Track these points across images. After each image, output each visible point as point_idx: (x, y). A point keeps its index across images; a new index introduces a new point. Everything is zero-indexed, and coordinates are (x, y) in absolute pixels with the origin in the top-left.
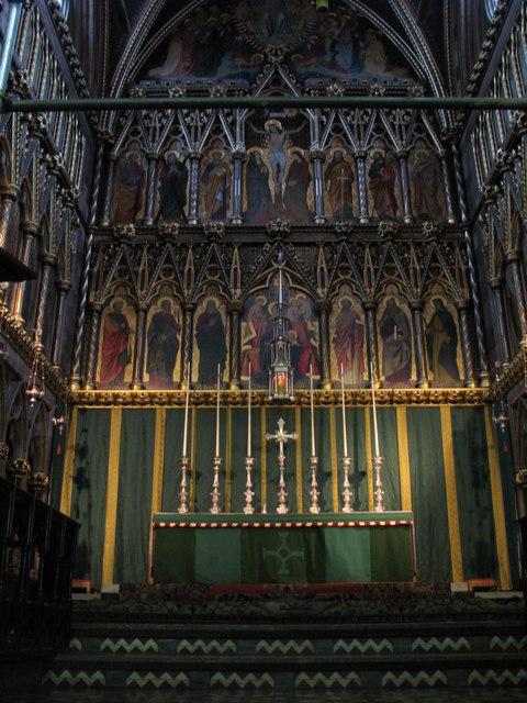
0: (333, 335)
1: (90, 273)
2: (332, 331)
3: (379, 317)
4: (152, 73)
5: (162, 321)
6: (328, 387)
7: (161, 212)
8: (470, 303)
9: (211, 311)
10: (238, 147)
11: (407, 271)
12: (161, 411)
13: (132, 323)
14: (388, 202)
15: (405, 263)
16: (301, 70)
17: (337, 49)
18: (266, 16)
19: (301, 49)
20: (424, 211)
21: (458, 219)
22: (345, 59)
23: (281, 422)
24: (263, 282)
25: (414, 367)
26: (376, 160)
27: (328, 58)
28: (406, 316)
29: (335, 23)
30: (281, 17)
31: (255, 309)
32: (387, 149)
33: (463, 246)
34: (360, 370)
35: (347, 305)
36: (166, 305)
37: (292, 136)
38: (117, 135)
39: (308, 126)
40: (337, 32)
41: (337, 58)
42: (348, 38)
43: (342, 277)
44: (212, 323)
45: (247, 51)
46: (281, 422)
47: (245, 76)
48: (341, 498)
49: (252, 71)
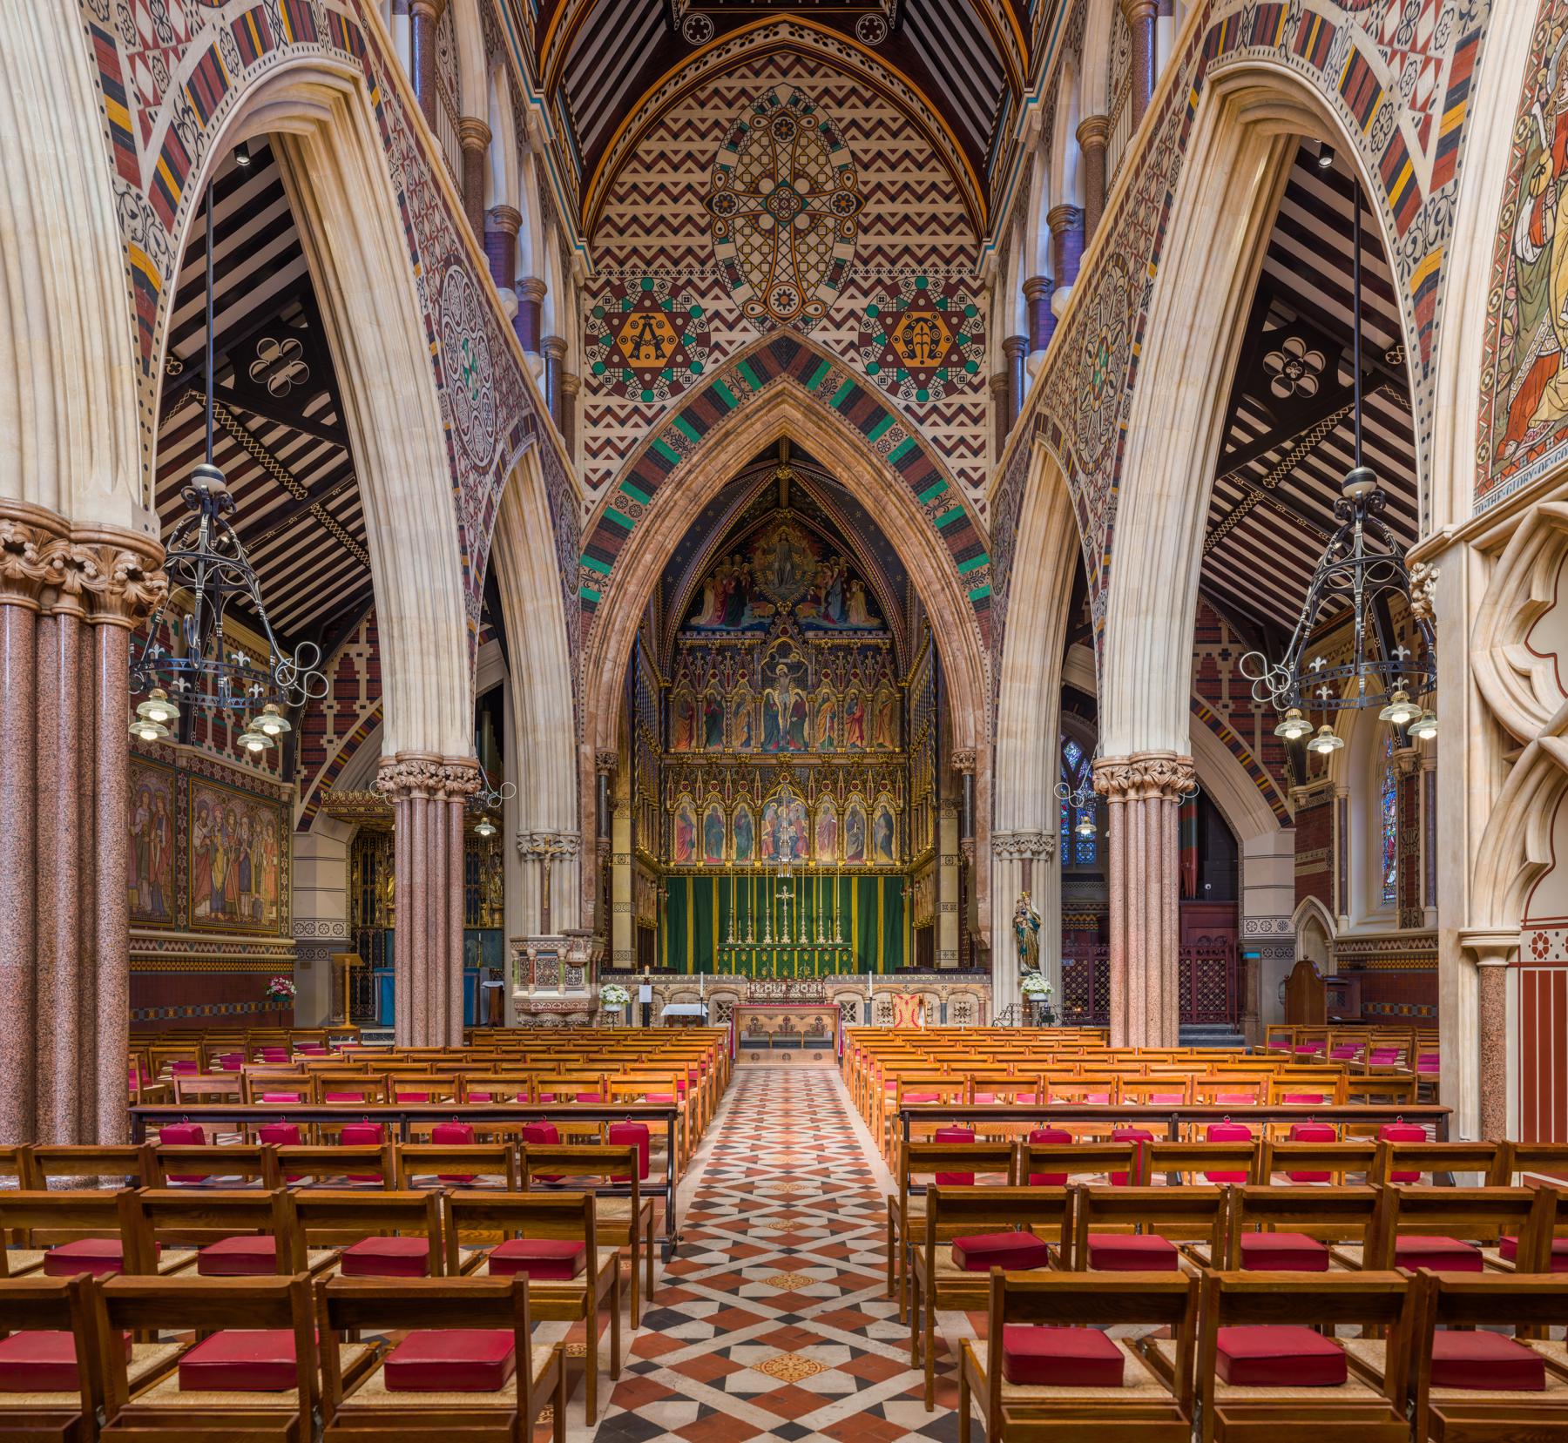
4: (694, 621)
5: (714, 819)
8: (903, 810)
12: (715, 880)
16: (802, 621)
18: (776, 565)
19: (803, 599)
22: (834, 611)
30: (789, 567)
34: (833, 852)
36: (715, 809)
37: (795, 680)
42: (838, 588)
45: (762, 598)
49: (767, 621)
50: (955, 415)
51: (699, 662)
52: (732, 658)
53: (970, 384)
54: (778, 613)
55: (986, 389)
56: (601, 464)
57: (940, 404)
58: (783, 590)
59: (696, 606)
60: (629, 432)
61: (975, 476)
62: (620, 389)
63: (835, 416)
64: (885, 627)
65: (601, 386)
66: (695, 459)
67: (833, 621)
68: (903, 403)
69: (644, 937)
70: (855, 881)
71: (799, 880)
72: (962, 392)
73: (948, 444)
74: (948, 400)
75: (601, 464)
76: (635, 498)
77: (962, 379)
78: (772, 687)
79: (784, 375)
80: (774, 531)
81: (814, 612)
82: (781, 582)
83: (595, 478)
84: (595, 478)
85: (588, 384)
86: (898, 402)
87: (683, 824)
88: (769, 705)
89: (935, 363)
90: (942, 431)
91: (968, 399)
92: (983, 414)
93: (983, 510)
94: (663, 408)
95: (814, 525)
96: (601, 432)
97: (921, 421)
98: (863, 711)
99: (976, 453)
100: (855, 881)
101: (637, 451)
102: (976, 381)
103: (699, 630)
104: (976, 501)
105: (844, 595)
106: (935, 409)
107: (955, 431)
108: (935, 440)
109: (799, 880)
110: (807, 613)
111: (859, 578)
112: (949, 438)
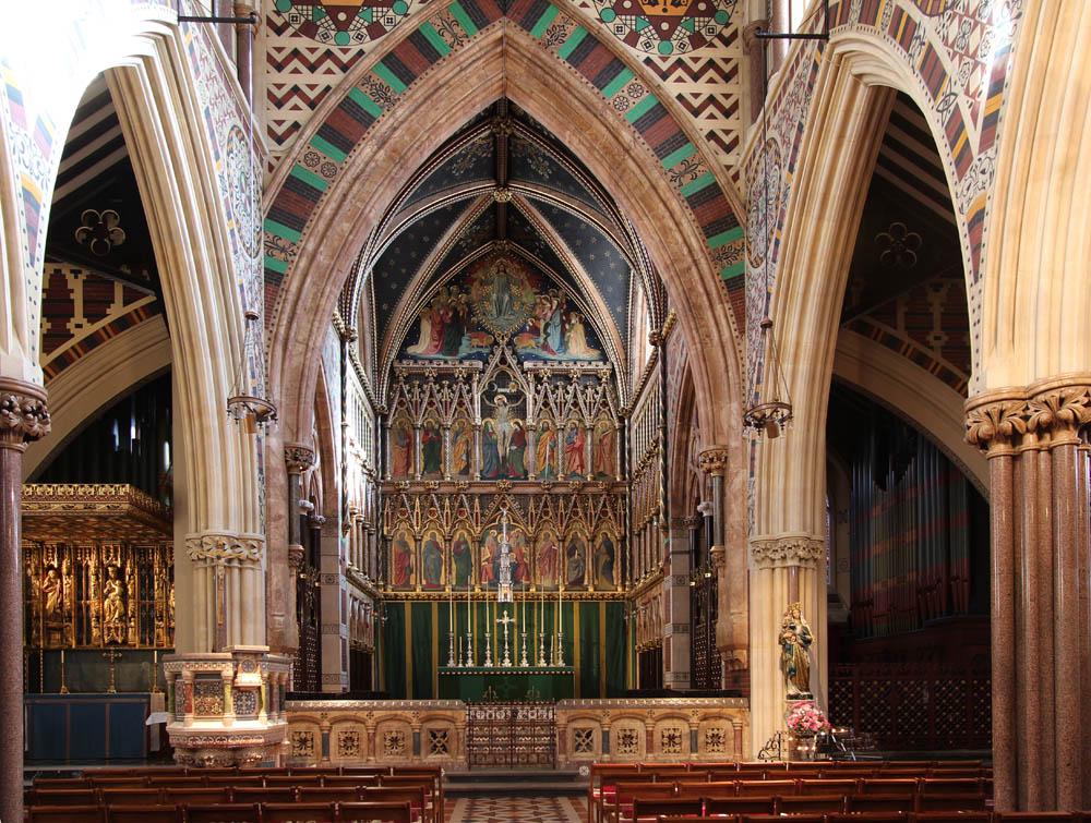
0: (538, 556)
1: (382, 514)
2: (537, 554)
3: (567, 544)
4: (411, 350)
6: (533, 590)
7: (424, 469)
9: (462, 539)
10: (478, 421)
11: (586, 515)
12: (435, 606)
13: (412, 545)
14: (577, 462)
15: (585, 509)
16: (520, 351)
17: (549, 331)
18: (494, 296)
19: (522, 330)
20: (601, 469)
21: (624, 479)
22: (554, 342)
23: (505, 613)
24: (494, 520)
25: (586, 576)
26: (572, 429)
27: (542, 340)
28: (583, 545)
29: (549, 305)
30: (507, 298)
31: (489, 539)
32: (580, 421)
33: (624, 497)
34: (554, 578)
35: (547, 536)
36: (433, 535)
38: (389, 409)
39: (525, 400)
40: (549, 314)
41: (549, 339)
42: (557, 320)
43: (545, 518)
44: (463, 547)
45: (479, 329)
46: (505, 613)
47: (479, 356)
48: (539, 655)
50: (703, 70)
51: (417, 391)
52: (450, 387)
53: (720, 36)
54: (496, 343)
55: (738, 42)
56: (288, 116)
57: (686, 58)
58: (502, 321)
59: (413, 336)
60: (321, 79)
61: (727, 140)
62: (309, 29)
63: (564, 68)
64: (605, 359)
65: (286, 25)
66: (401, 112)
67: (553, 352)
68: (644, 56)
69: (359, 661)
70: (576, 606)
71: (520, 605)
72: (712, 45)
73: (696, 103)
74: (695, 54)
75: (288, 116)
76: (331, 154)
77: (711, 31)
78: (490, 416)
79: (505, 19)
80: (492, 262)
81: (533, 343)
82: (500, 312)
83: (280, 130)
84: (280, 130)
85: (270, 23)
86: (637, 54)
87: (401, 550)
88: (487, 433)
89: (681, 11)
90: (688, 88)
91: (718, 53)
92: (735, 71)
93: (736, 177)
94: (361, 53)
95: (531, 257)
96: (287, 78)
97: (664, 76)
98: (583, 441)
99: (727, 113)
100: (576, 606)
101: (333, 101)
102: (727, 33)
103: (415, 359)
104: (728, 167)
105: (563, 328)
106: (680, 63)
107: (703, 88)
108: (680, 97)
109: (520, 605)
110: (527, 344)
111: (576, 309)
112: (696, 96)
